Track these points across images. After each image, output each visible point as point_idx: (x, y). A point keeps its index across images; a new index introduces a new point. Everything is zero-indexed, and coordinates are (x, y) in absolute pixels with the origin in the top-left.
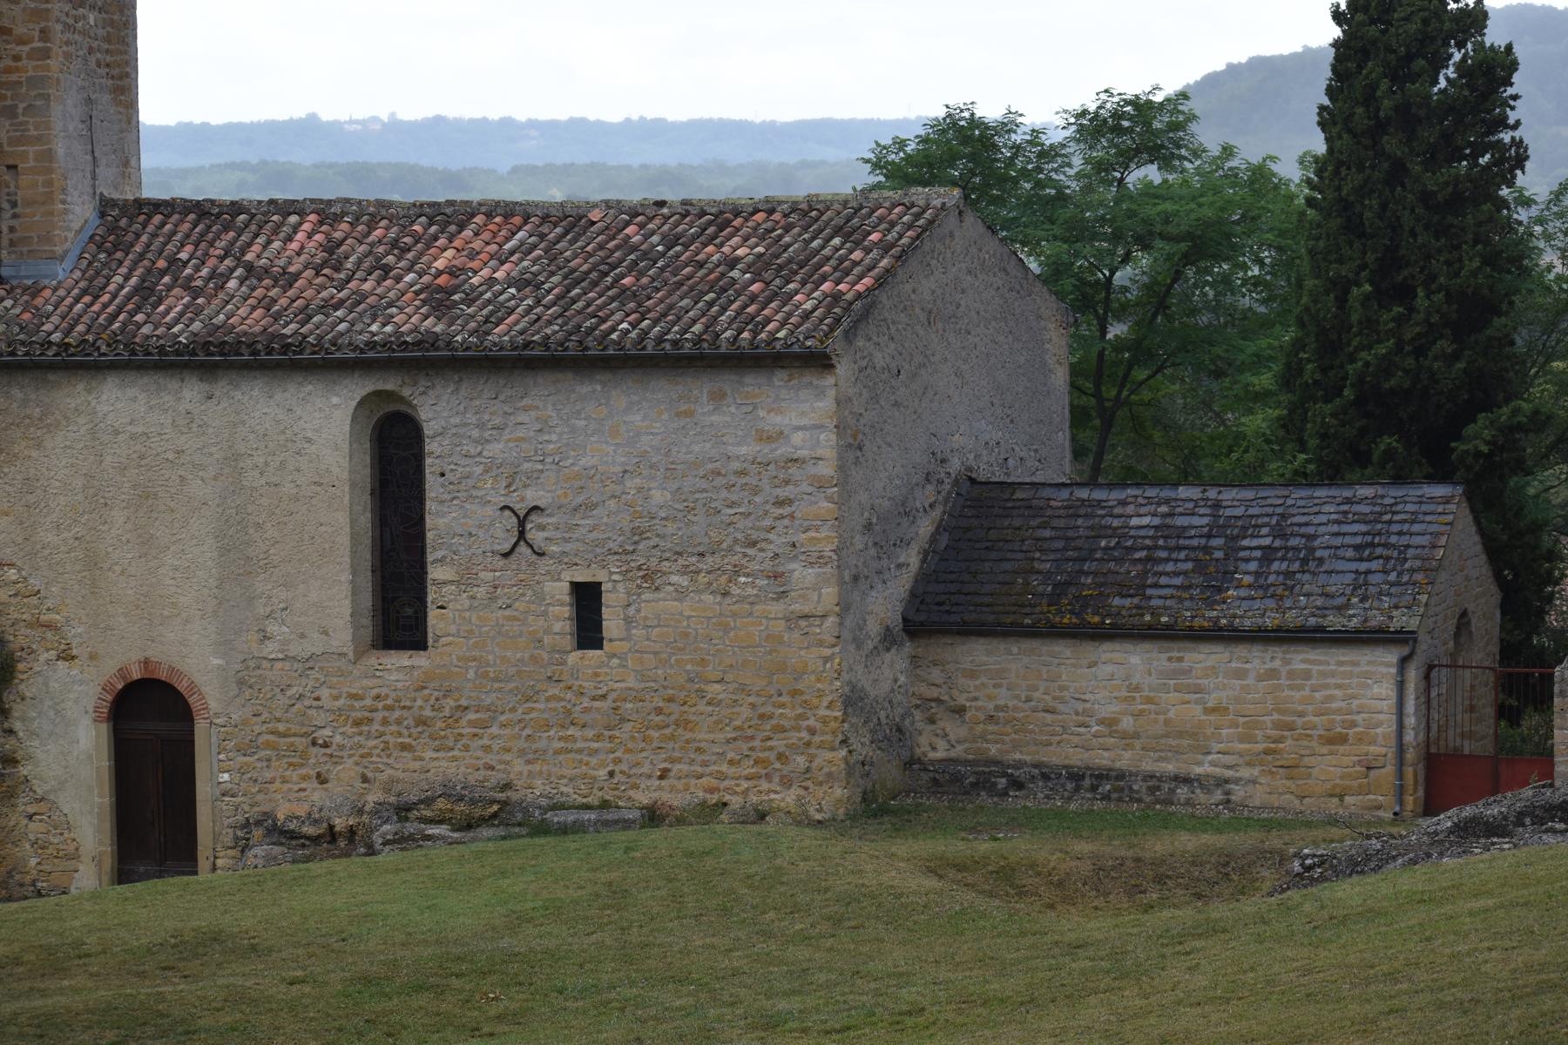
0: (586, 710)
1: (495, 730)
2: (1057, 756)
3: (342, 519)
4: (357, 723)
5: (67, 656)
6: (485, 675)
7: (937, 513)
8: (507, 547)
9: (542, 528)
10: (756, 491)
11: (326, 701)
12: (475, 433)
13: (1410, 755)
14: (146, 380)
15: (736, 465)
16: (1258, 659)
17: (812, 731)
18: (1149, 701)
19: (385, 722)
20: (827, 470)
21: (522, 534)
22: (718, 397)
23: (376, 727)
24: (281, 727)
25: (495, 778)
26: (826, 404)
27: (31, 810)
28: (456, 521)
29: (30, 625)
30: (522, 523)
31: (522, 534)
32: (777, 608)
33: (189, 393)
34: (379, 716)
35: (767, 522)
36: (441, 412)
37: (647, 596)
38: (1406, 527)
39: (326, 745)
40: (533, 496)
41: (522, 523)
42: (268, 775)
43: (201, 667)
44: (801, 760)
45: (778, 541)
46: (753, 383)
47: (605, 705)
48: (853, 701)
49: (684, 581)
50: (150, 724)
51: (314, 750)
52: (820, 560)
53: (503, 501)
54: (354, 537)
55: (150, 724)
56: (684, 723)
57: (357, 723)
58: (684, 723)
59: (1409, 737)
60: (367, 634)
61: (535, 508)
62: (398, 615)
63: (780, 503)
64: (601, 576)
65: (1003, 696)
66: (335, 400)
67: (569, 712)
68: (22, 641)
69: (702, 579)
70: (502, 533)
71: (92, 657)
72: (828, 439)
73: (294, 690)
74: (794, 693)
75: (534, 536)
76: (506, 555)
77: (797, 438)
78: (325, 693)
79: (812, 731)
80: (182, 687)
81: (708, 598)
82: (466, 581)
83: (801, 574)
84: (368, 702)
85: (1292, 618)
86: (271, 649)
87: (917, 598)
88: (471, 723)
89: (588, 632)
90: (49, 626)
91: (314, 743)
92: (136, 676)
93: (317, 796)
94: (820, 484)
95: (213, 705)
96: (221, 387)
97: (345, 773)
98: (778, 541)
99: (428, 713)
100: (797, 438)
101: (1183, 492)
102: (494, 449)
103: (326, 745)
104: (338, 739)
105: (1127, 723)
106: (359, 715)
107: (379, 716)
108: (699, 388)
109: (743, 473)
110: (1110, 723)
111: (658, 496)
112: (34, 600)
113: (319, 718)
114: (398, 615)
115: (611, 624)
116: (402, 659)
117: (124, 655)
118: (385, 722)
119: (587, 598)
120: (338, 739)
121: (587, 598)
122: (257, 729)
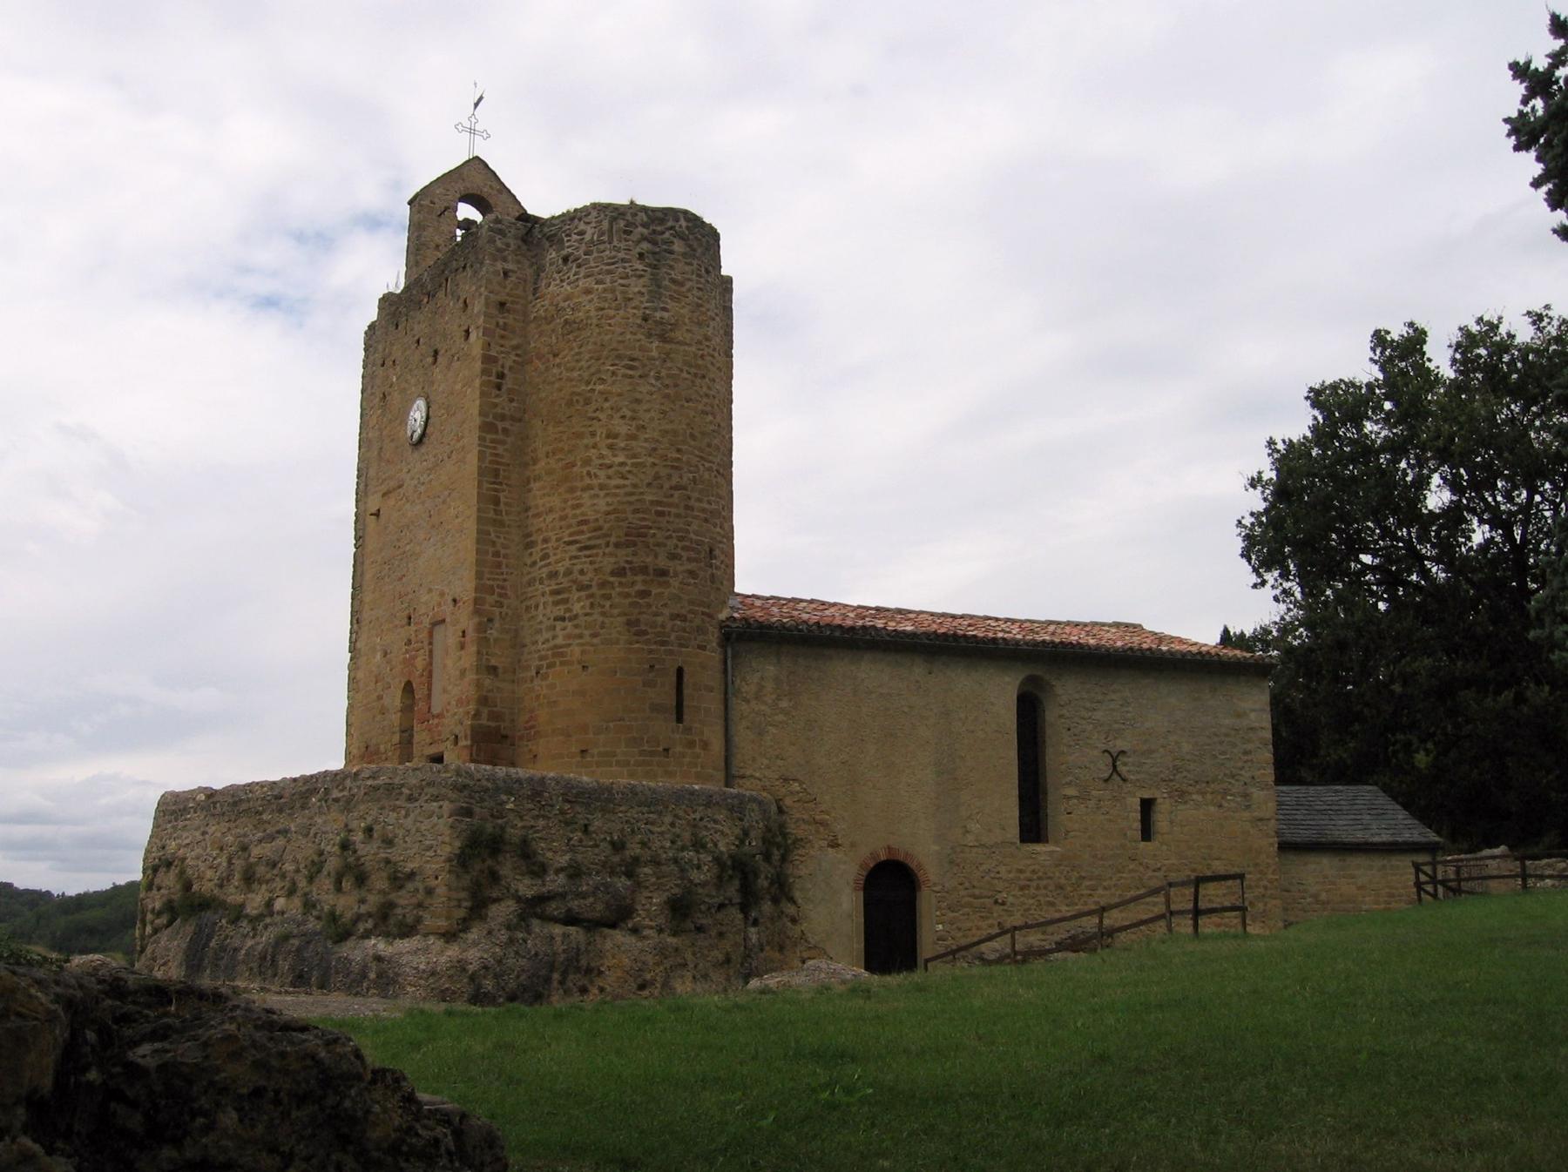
0: (1150, 878)
1: (1100, 891)
4: (1022, 888)
5: (834, 845)
6: (1095, 856)
8: (1106, 775)
9: (1125, 764)
10: (1234, 745)
11: (1003, 875)
12: (1088, 705)
15: (1223, 730)
17: (1266, 888)
18: (1334, 883)
19: (1038, 888)
21: (1115, 767)
23: (1033, 891)
24: (977, 892)
26: (1265, 698)
27: (805, 955)
29: (808, 823)
30: (1114, 761)
31: (1115, 767)
32: (1246, 814)
33: (917, 670)
34: (1034, 884)
35: (1240, 764)
37: (1181, 807)
39: (1003, 904)
40: (1121, 744)
41: (1114, 761)
42: (969, 925)
43: (926, 854)
44: (1261, 905)
47: (1160, 874)
49: (1199, 798)
50: (891, 891)
51: (997, 908)
53: (1104, 747)
55: (891, 891)
57: (1022, 888)
61: (1123, 752)
63: (1246, 753)
64: (1157, 795)
66: (1007, 679)
67: (1141, 879)
68: (800, 833)
69: (1209, 797)
71: (853, 845)
72: (1267, 717)
73: (984, 867)
74: (1256, 865)
75: (1122, 769)
76: (1106, 781)
77: (1253, 715)
78: (1003, 869)
79: (1266, 888)
80: (913, 866)
81: (1212, 809)
83: (1257, 794)
84: (1028, 874)
86: (970, 840)
88: (1088, 888)
90: (822, 823)
91: (996, 902)
92: (883, 858)
95: (933, 878)
98: (1246, 775)
99: (1063, 881)
100: (1253, 715)
102: (1098, 715)
103: (1003, 904)
104: (1011, 899)
105: (1323, 896)
106: (1022, 883)
107: (1034, 884)
109: (1227, 735)
110: (1315, 896)
111: (1186, 747)
112: (811, 805)
113: (1000, 885)
117: (873, 845)
118: (1038, 888)
119: (1147, 806)
120: (1011, 899)
121: (1147, 806)
122: (962, 893)
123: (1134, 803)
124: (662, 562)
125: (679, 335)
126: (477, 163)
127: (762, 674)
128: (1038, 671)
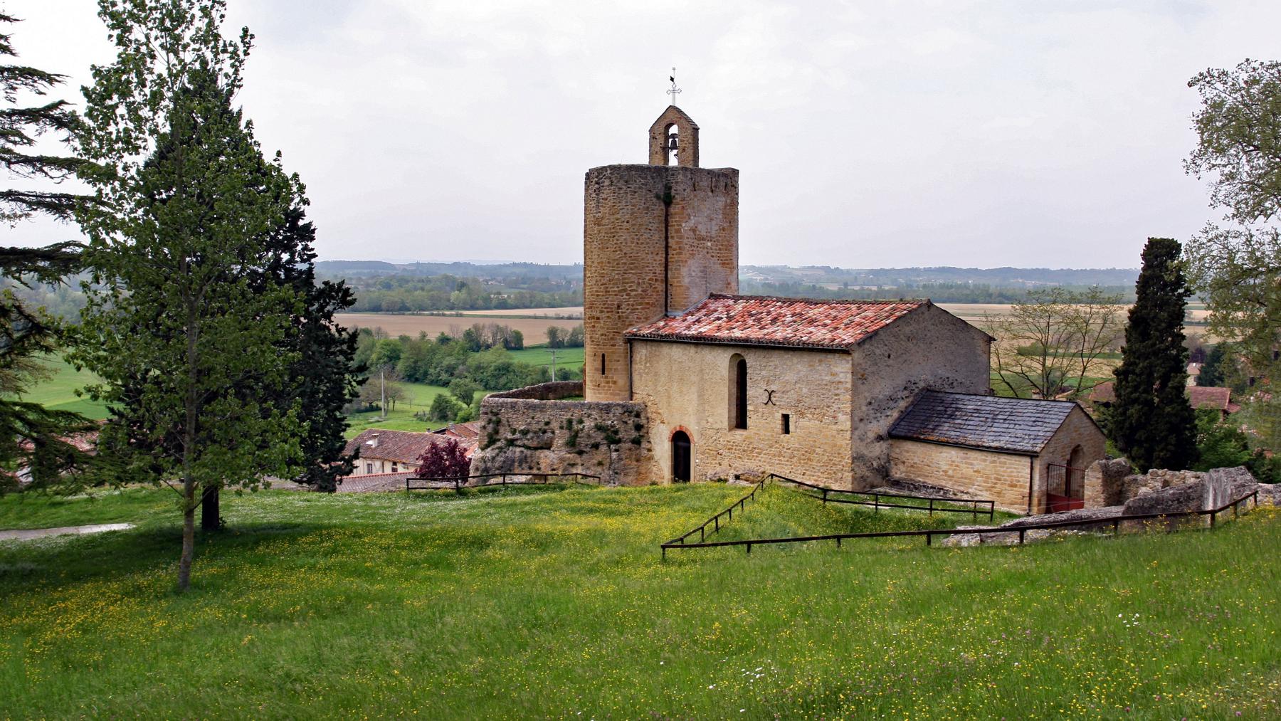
2: (930, 482)
3: (726, 390)
7: (911, 399)
13: (1035, 494)
14: (683, 346)
16: (990, 457)
20: (849, 386)
22: (820, 361)
25: (762, 469)
26: (849, 366)
28: (755, 393)
33: (692, 350)
36: (752, 360)
38: (58, 498)
40: (773, 387)
43: (693, 430)
45: (835, 407)
46: (830, 356)
48: (857, 458)
50: (681, 441)
52: (846, 414)
54: (730, 395)
55: (681, 441)
56: (809, 459)
58: (809, 459)
59: (1036, 488)
60: (734, 423)
62: (741, 421)
65: (916, 460)
70: (765, 398)
72: (849, 376)
82: (756, 411)
85: (1001, 444)
87: (896, 424)
89: (786, 430)
93: (718, 469)
94: (847, 390)
96: (699, 349)
97: (725, 463)
98: (835, 407)
101: (989, 398)
102: (763, 373)
105: (950, 472)
108: (816, 358)
110: (945, 472)
111: (805, 390)
114: (741, 421)
115: (792, 428)
116: (740, 432)
117: (675, 425)
119: (786, 418)
121: (786, 418)
123: (779, 416)
124: (598, 315)
125: (603, 222)
126: (672, 109)
127: (641, 352)
128: (739, 351)
